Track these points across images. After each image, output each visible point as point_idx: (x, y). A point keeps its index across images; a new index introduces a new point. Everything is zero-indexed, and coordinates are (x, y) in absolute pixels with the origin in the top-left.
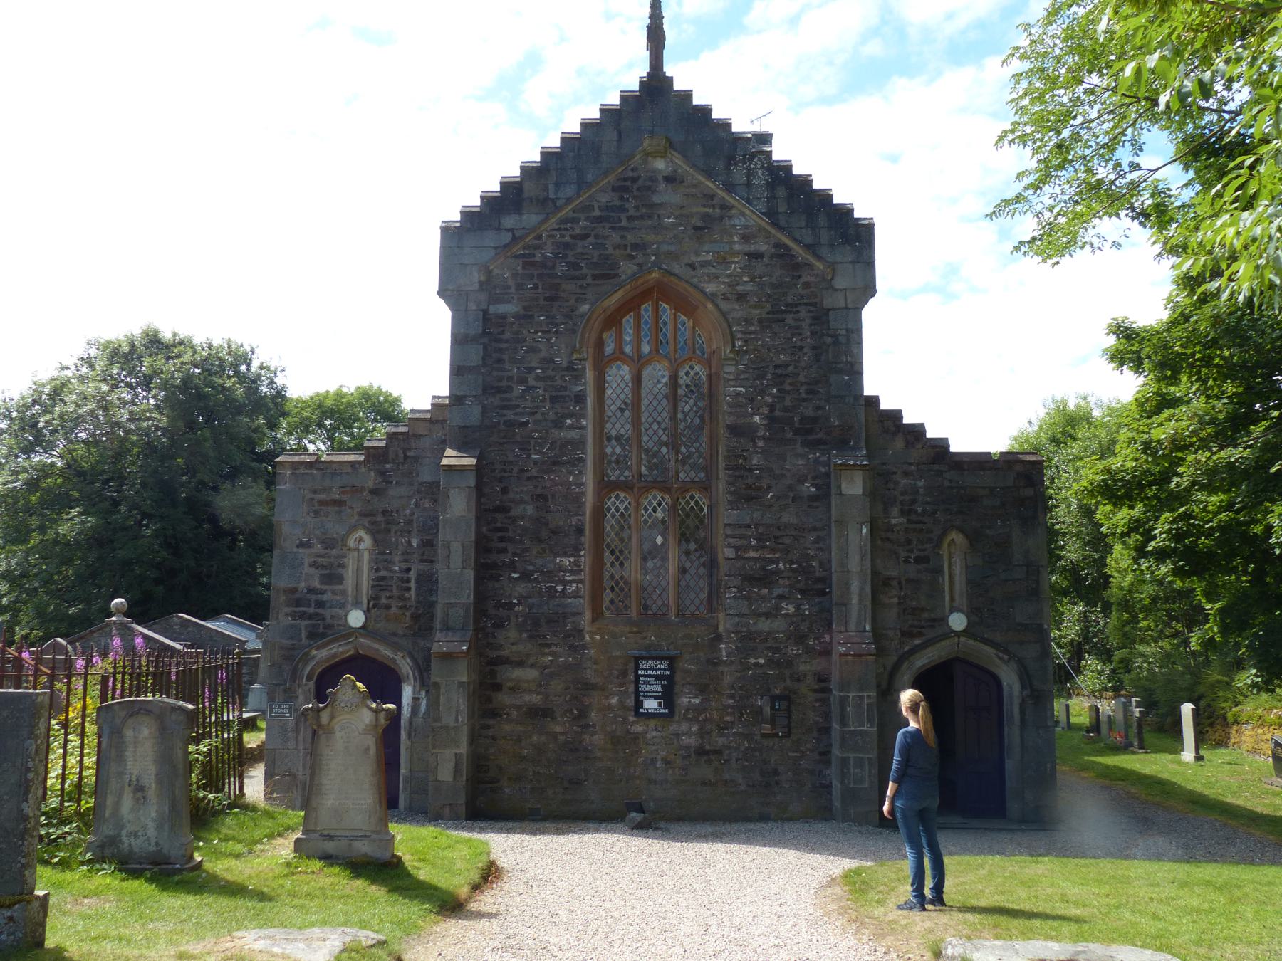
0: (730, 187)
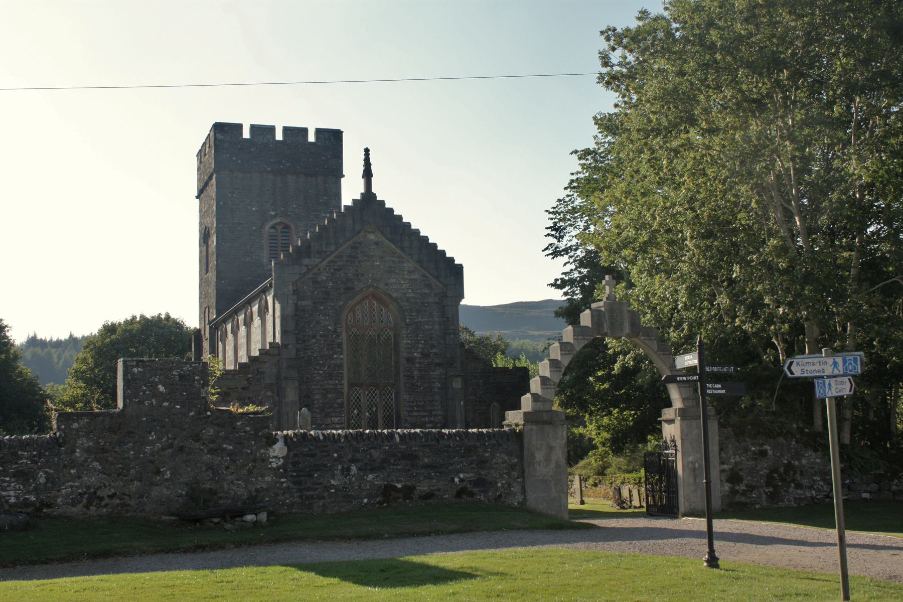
0: (403, 249)
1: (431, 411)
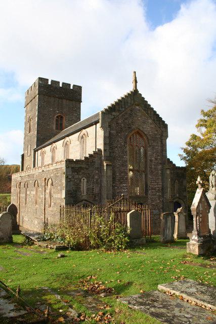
0: (148, 114)
1: (158, 183)
